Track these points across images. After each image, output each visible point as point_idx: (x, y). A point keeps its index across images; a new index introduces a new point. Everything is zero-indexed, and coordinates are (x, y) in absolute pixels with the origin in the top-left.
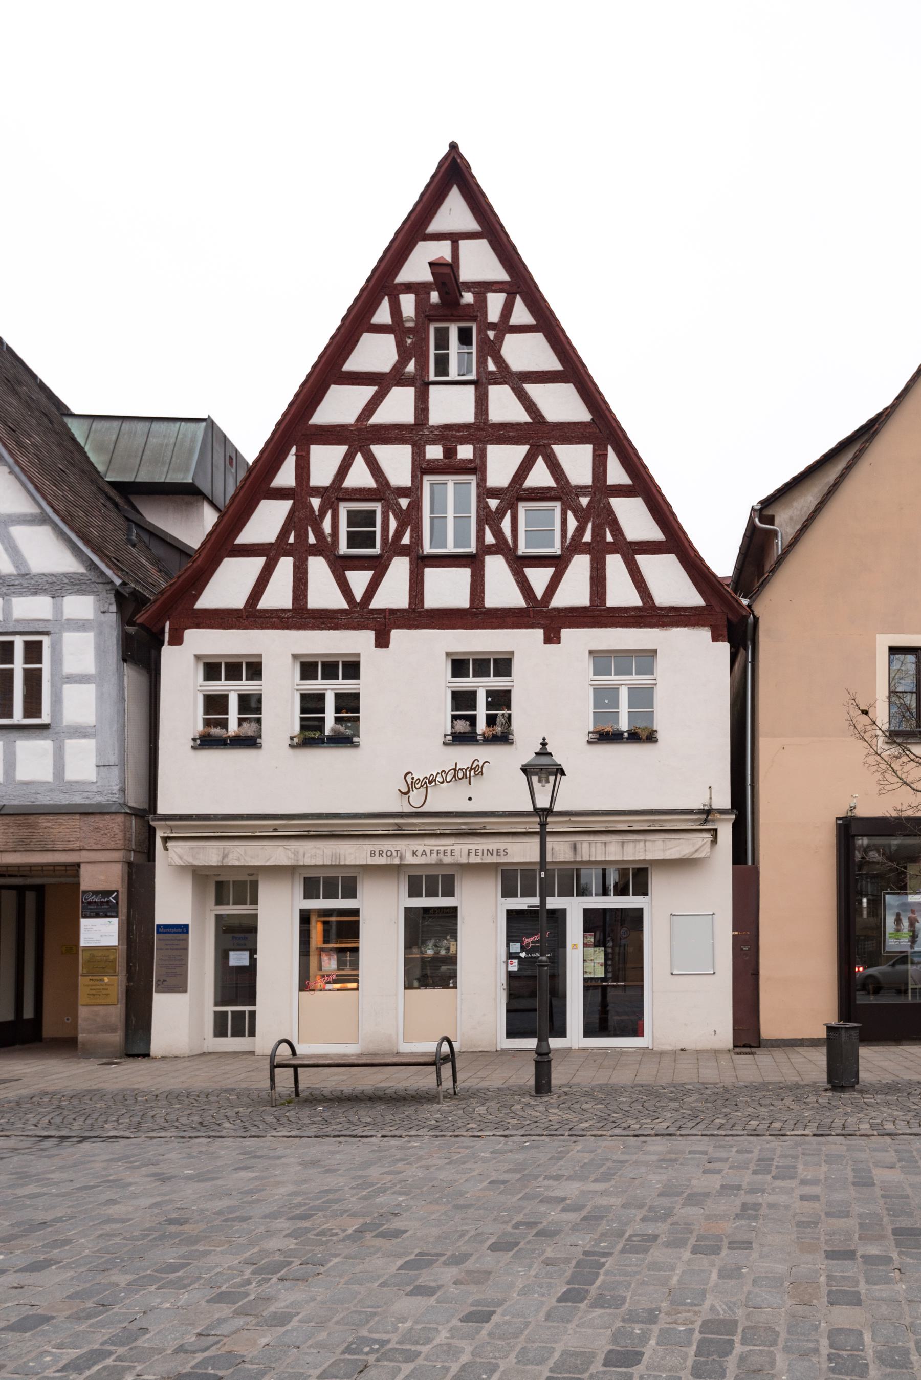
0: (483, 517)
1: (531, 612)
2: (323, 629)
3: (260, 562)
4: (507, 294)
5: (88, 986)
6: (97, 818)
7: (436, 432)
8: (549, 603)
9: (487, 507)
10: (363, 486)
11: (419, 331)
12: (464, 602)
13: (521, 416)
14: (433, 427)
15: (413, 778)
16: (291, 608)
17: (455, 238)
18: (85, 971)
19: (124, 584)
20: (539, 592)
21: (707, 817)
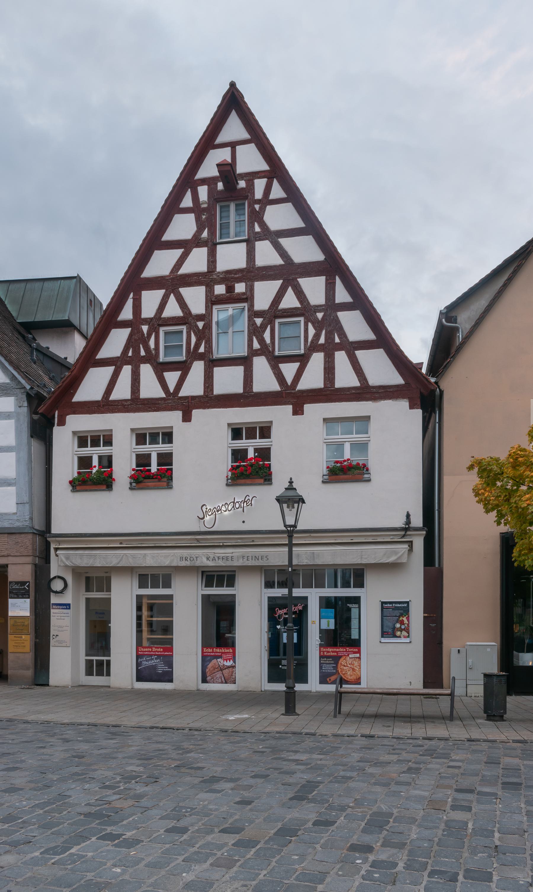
0: (252, 331)
1: (284, 394)
2: (150, 411)
3: (110, 370)
4: (268, 178)
5: (13, 640)
6: (17, 536)
7: (221, 276)
8: (296, 387)
10: (174, 316)
13: (277, 260)
14: (219, 272)
15: (207, 509)
16: (130, 398)
17: (233, 145)
18: (11, 631)
19: (32, 388)
20: (289, 380)
21: (406, 533)
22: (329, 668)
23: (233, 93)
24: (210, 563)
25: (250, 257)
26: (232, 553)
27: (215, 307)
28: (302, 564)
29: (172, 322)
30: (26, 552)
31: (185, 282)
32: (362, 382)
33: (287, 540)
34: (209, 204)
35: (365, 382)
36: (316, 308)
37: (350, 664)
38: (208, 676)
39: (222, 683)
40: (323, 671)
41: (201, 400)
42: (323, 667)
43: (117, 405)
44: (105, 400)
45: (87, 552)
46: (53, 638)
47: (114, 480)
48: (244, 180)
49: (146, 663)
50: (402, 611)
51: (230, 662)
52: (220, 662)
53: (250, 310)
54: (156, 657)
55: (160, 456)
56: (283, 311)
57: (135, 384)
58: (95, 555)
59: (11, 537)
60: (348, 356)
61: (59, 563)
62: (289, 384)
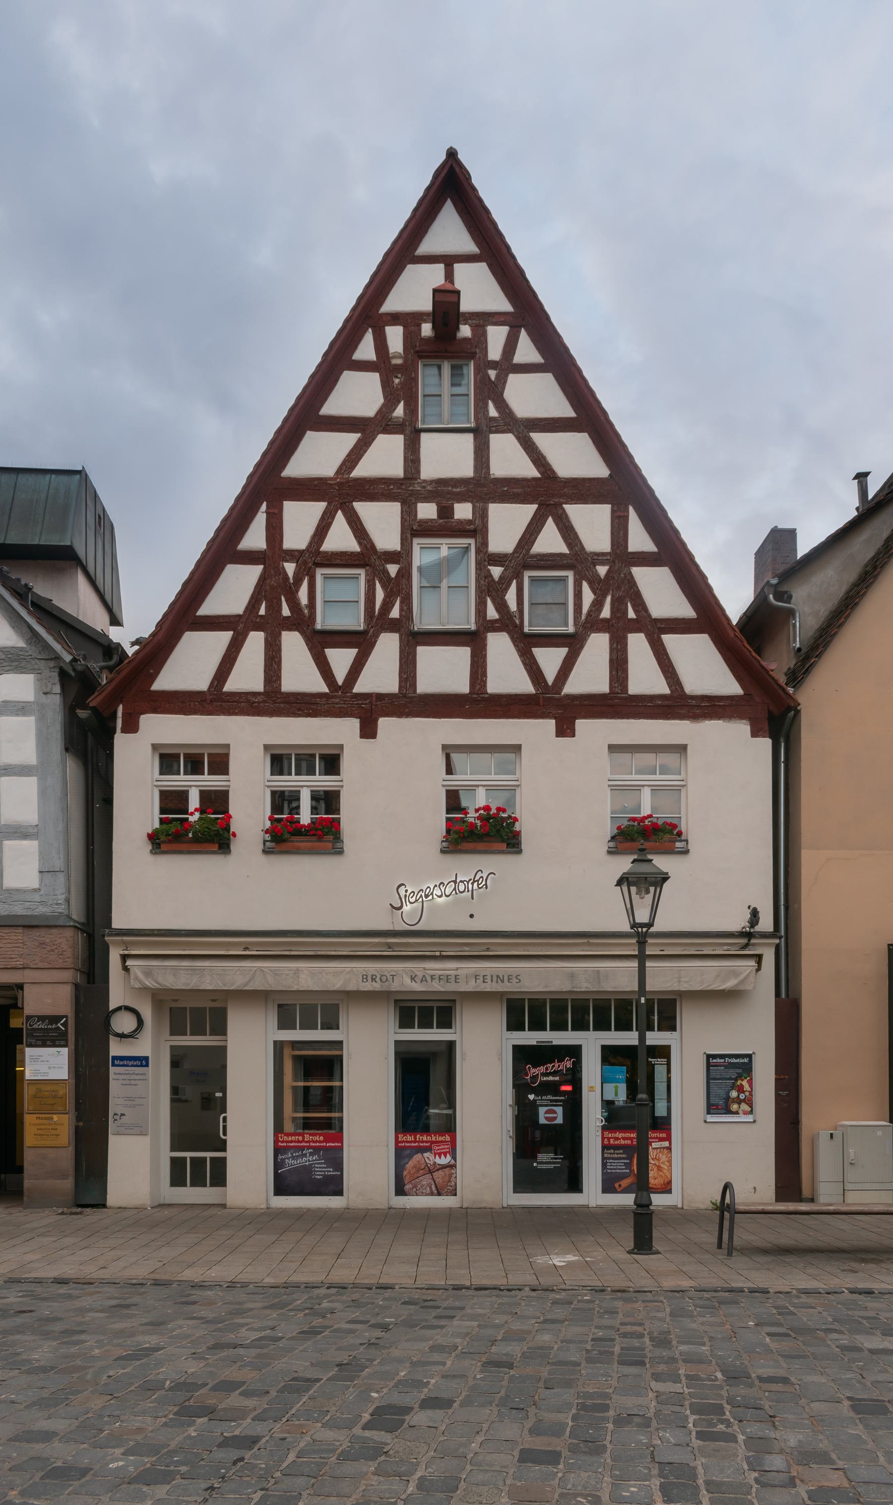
0: (484, 588)
1: (541, 700)
2: (299, 716)
3: (226, 636)
4: (511, 327)
5: (35, 1125)
6: (43, 932)
7: (429, 488)
8: (561, 689)
9: (489, 575)
10: (344, 550)
11: (408, 370)
12: (464, 687)
13: (529, 470)
14: (425, 481)
15: (406, 891)
16: (263, 691)
17: (449, 261)
18: (31, 1108)
19: (75, 660)
22: (618, 1166)
23: (451, 170)
24: (417, 987)
25: (480, 459)
26: (457, 969)
27: (416, 541)
28: (579, 990)
29: (341, 560)
30: (60, 961)
31: (363, 491)
32: (673, 688)
33: (637, 948)
34: (405, 359)
35: (677, 687)
36: (596, 557)
37: (653, 1159)
38: (406, 1182)
39: (432, 1194)
40: (609, 1171)
41: (394, 702)
42: (608, 1164)
43: (238, 702)
44: (214, 691)
45: (185, 963)
46: (115, 1120)
47: (234, 835)
48: (469, 325)
49: (291, 1162)
50: (740, 1071)
51: (446, 1158)
52: (428, 1158)
53: (481, 551)
54: (311, 1150)
55: (205, 795)
56: (538, 557)
57: (272, 665)
58: (202, 970)
59: (30, 933)
60: (649, 642)
61: (132, 983)
62: (550, 682)
